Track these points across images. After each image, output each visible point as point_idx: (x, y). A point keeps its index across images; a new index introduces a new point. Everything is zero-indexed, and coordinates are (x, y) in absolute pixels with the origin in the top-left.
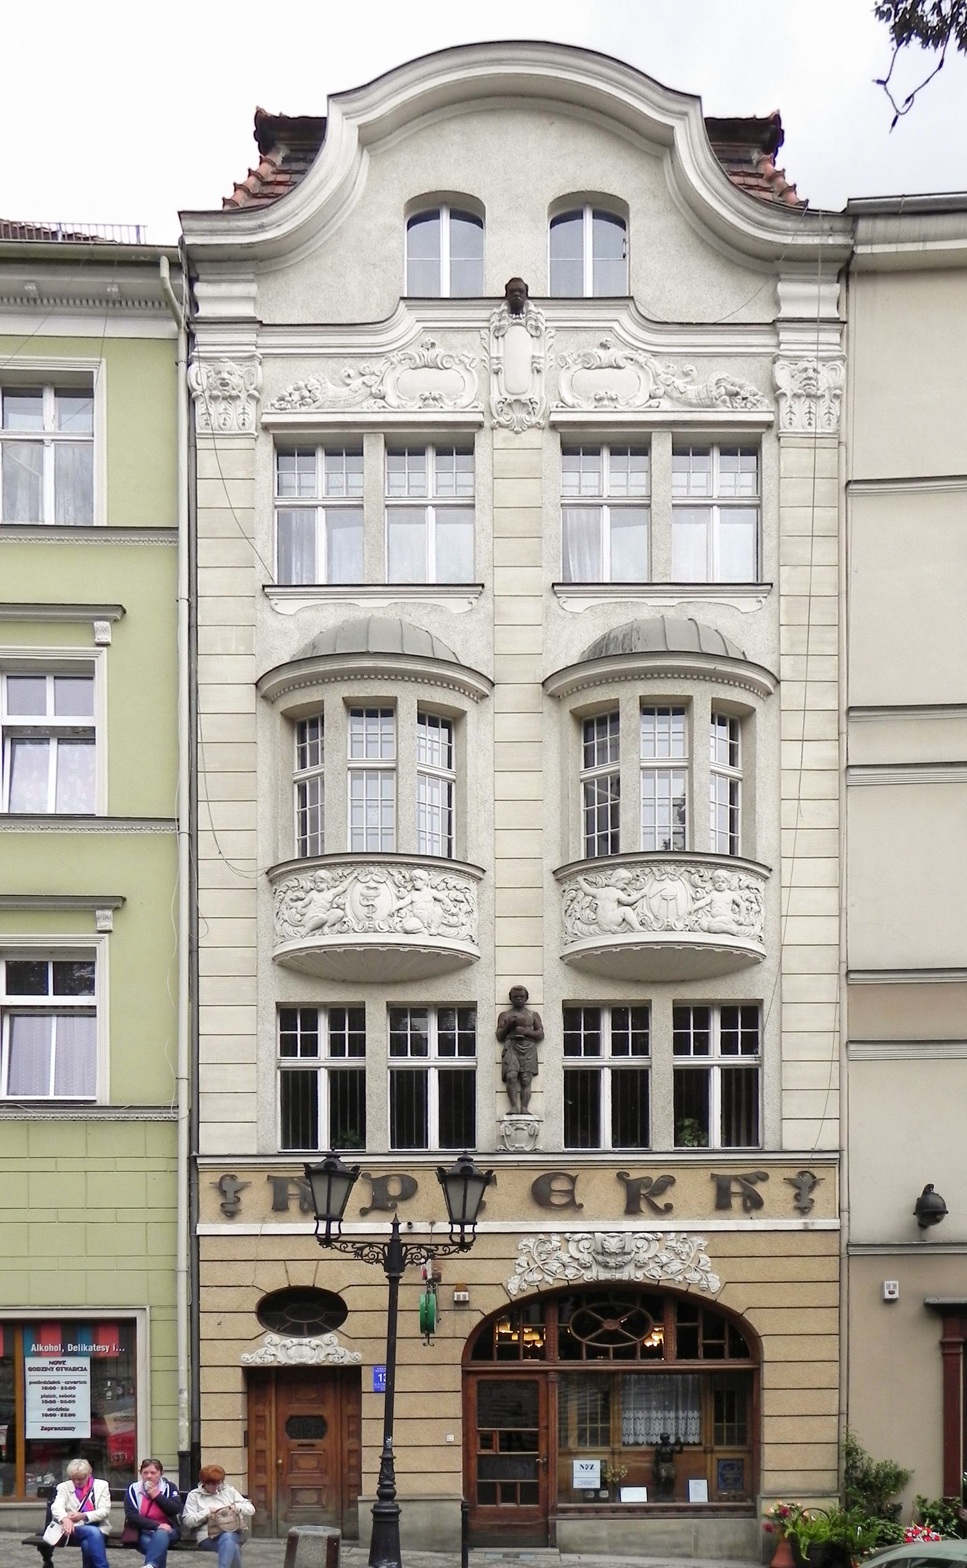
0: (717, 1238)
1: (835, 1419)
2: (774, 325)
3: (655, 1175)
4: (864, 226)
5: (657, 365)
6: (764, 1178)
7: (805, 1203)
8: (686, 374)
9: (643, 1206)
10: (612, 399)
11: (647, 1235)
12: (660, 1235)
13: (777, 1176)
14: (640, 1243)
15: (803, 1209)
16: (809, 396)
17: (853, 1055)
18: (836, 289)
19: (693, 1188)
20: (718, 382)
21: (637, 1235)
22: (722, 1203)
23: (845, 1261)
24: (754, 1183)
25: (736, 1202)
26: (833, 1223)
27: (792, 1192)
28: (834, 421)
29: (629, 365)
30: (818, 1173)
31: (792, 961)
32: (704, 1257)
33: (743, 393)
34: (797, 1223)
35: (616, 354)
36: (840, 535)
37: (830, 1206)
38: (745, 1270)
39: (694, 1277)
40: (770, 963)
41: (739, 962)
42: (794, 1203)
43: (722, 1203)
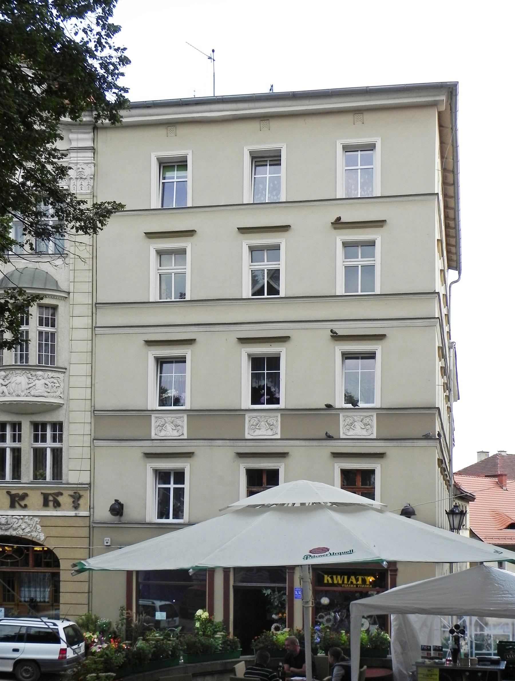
0: (43, 518)
1: (87, 594)
3: (21, 492)
6: (61, 494)
7: (77, 506)
9: (17, 505)
11: (17, 517)
12: (22, 517)
13: (66, 493)
14: (15, 520)
15: (76, 507)
17: (96, 444)
19: (35, 498)
21: (14, 517)
22: (46, 504)
24: (58, 496)
25: (51, 504)
26: (86, 513)
27: (72, 500)
28: (90, 187)
30: (81, 493)
32: (39, 526)
34: (73, 513)
38: (54, 532)
39: (34, 534)
40: (65, 407)
41: (55, 407)
42: (73, 505)
43: (46, 504)
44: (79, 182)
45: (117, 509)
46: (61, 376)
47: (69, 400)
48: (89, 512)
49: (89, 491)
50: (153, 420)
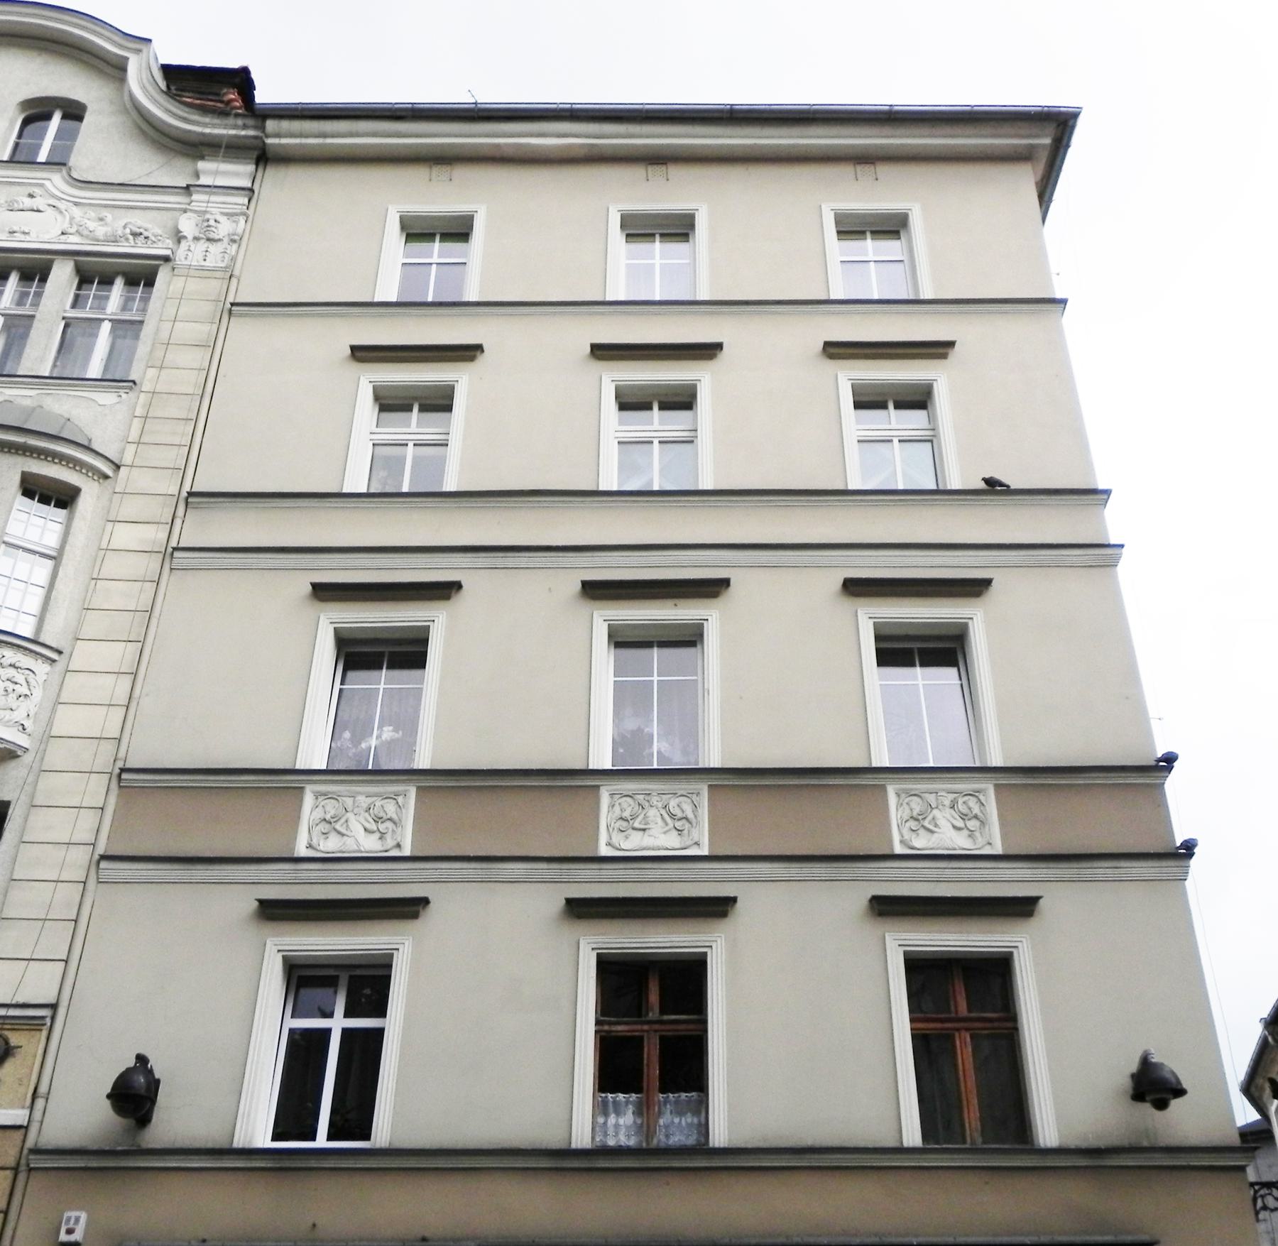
2: (188, 187)
4: (271, 125)
5: (77, 212)
8: (101, 219)
10: (24, 233)
16: (209, 240)
18: (251, 168)
20: (125, 227)
23: (22, 1177)
29: (50, 210)
30: (15, 1039)
31: (57, 755)
33: (146, 234)
35: (38, 202)
36: (212, 346)
37: (22, 1090)
40: (27, 759)
44: (202, 245)
45: (134, 1095)
46: (41, 668)
47: (48, 737)
48: (27, 1112)
49: (44, 1033)
50: (308, 799)
